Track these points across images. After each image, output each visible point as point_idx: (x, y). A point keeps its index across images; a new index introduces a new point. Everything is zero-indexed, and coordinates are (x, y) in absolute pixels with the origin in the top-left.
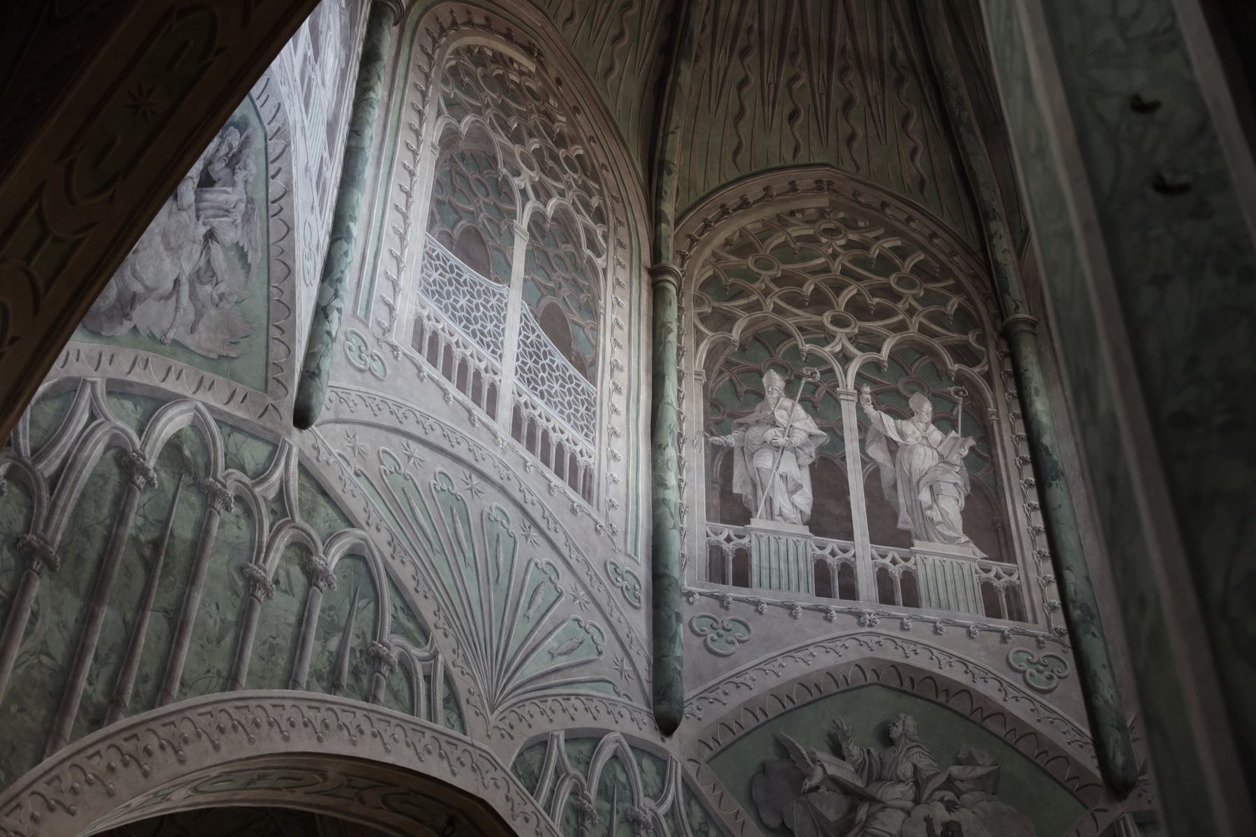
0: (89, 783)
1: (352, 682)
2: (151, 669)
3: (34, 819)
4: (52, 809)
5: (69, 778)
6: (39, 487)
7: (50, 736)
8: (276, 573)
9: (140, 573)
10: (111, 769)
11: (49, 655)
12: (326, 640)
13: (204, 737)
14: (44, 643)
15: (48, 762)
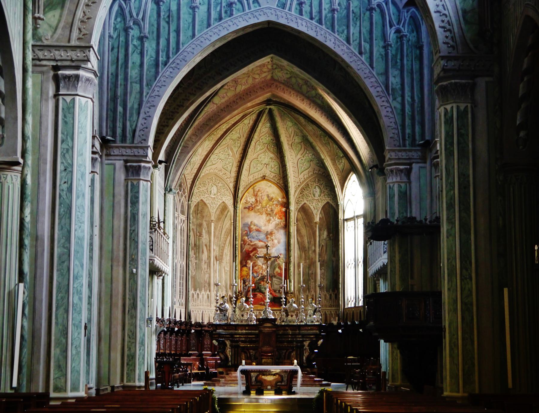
0: (167, 78)
1: (225, 15)
2: (174, 46)
3: (158, 91)
4: (161, 87)
5: (162, 79)
6: (140, 22)
7: (157, 73)
8: (199, 1)
9: (166, 26)
10: (171, 72)
11: (152, 57)
12: (216, 9)
13: (190, 53)
14: (151, 55)
15: (158, 79)
